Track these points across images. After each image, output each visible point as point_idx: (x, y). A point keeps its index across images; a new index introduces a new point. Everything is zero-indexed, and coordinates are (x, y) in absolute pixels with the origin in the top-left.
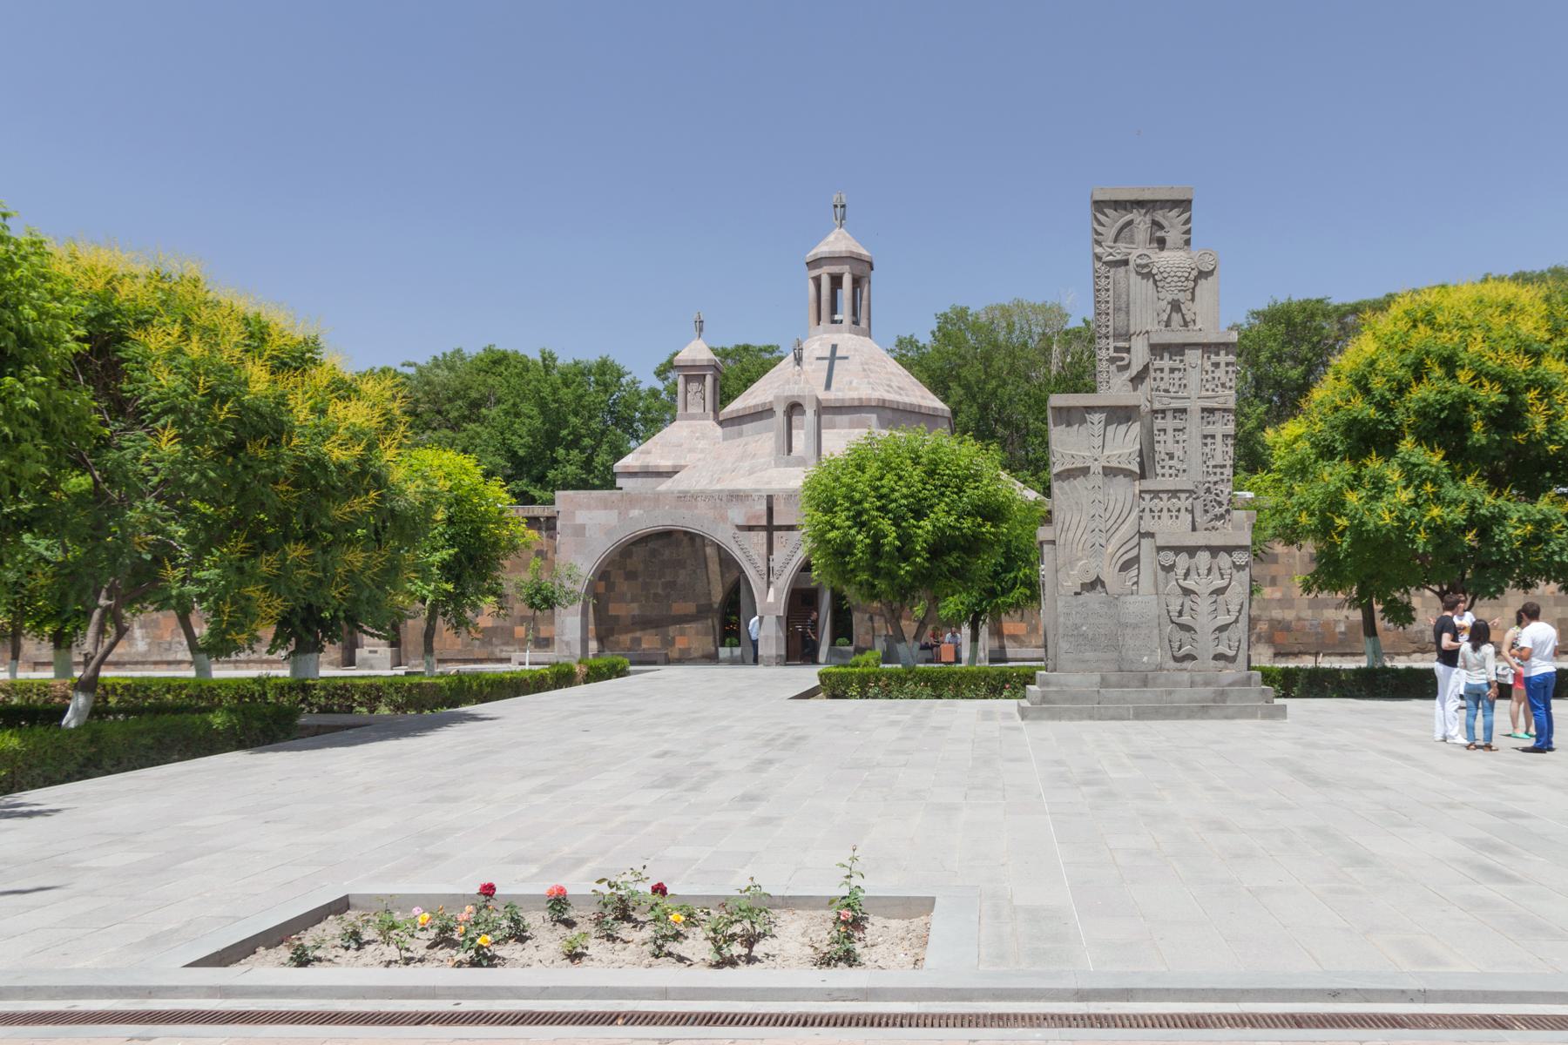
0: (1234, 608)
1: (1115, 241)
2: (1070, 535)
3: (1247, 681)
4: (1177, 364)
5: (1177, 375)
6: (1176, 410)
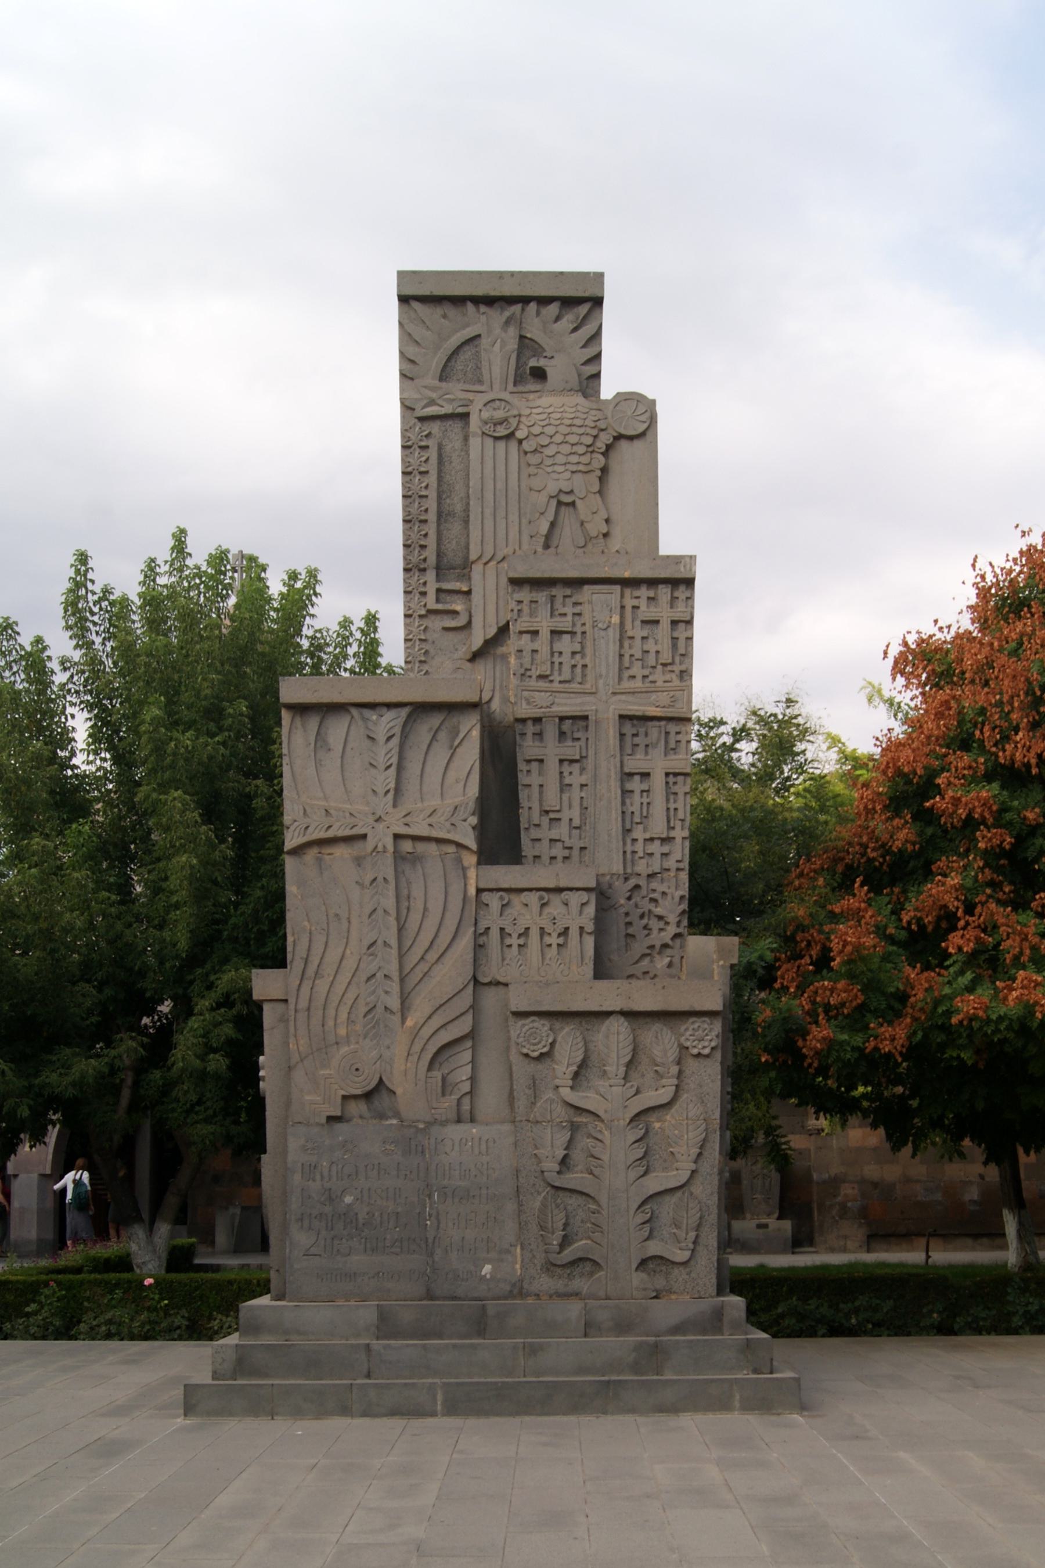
0: (685, 1152)
1: (444, 376)
2: (322, 986)
3: (715, 1321)
4: (565, 624)
5: (565, 644)
6: (562, 719)
